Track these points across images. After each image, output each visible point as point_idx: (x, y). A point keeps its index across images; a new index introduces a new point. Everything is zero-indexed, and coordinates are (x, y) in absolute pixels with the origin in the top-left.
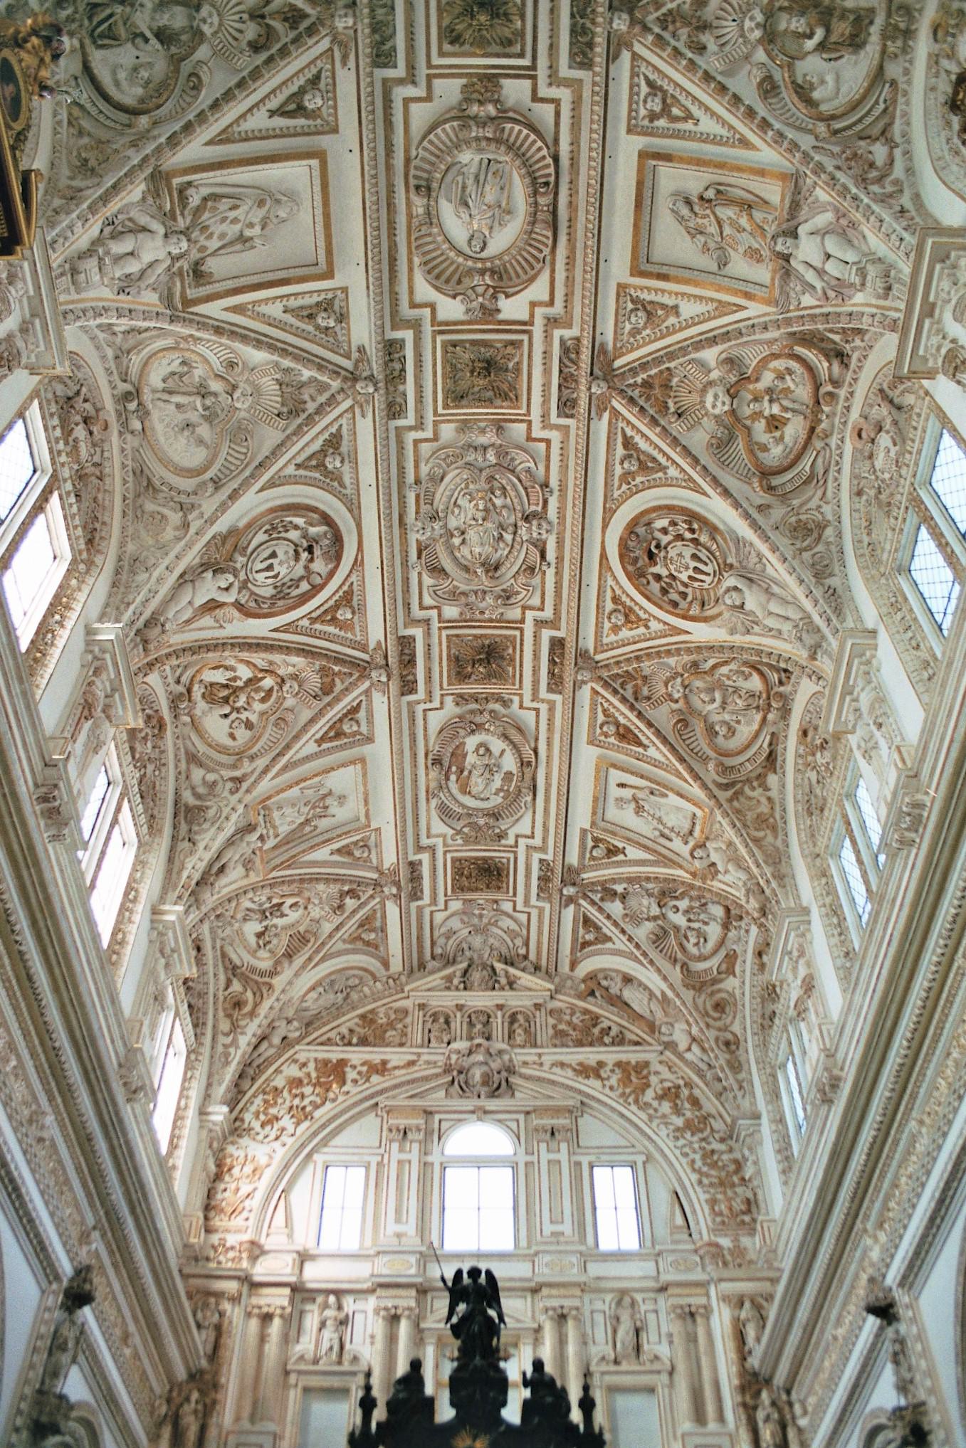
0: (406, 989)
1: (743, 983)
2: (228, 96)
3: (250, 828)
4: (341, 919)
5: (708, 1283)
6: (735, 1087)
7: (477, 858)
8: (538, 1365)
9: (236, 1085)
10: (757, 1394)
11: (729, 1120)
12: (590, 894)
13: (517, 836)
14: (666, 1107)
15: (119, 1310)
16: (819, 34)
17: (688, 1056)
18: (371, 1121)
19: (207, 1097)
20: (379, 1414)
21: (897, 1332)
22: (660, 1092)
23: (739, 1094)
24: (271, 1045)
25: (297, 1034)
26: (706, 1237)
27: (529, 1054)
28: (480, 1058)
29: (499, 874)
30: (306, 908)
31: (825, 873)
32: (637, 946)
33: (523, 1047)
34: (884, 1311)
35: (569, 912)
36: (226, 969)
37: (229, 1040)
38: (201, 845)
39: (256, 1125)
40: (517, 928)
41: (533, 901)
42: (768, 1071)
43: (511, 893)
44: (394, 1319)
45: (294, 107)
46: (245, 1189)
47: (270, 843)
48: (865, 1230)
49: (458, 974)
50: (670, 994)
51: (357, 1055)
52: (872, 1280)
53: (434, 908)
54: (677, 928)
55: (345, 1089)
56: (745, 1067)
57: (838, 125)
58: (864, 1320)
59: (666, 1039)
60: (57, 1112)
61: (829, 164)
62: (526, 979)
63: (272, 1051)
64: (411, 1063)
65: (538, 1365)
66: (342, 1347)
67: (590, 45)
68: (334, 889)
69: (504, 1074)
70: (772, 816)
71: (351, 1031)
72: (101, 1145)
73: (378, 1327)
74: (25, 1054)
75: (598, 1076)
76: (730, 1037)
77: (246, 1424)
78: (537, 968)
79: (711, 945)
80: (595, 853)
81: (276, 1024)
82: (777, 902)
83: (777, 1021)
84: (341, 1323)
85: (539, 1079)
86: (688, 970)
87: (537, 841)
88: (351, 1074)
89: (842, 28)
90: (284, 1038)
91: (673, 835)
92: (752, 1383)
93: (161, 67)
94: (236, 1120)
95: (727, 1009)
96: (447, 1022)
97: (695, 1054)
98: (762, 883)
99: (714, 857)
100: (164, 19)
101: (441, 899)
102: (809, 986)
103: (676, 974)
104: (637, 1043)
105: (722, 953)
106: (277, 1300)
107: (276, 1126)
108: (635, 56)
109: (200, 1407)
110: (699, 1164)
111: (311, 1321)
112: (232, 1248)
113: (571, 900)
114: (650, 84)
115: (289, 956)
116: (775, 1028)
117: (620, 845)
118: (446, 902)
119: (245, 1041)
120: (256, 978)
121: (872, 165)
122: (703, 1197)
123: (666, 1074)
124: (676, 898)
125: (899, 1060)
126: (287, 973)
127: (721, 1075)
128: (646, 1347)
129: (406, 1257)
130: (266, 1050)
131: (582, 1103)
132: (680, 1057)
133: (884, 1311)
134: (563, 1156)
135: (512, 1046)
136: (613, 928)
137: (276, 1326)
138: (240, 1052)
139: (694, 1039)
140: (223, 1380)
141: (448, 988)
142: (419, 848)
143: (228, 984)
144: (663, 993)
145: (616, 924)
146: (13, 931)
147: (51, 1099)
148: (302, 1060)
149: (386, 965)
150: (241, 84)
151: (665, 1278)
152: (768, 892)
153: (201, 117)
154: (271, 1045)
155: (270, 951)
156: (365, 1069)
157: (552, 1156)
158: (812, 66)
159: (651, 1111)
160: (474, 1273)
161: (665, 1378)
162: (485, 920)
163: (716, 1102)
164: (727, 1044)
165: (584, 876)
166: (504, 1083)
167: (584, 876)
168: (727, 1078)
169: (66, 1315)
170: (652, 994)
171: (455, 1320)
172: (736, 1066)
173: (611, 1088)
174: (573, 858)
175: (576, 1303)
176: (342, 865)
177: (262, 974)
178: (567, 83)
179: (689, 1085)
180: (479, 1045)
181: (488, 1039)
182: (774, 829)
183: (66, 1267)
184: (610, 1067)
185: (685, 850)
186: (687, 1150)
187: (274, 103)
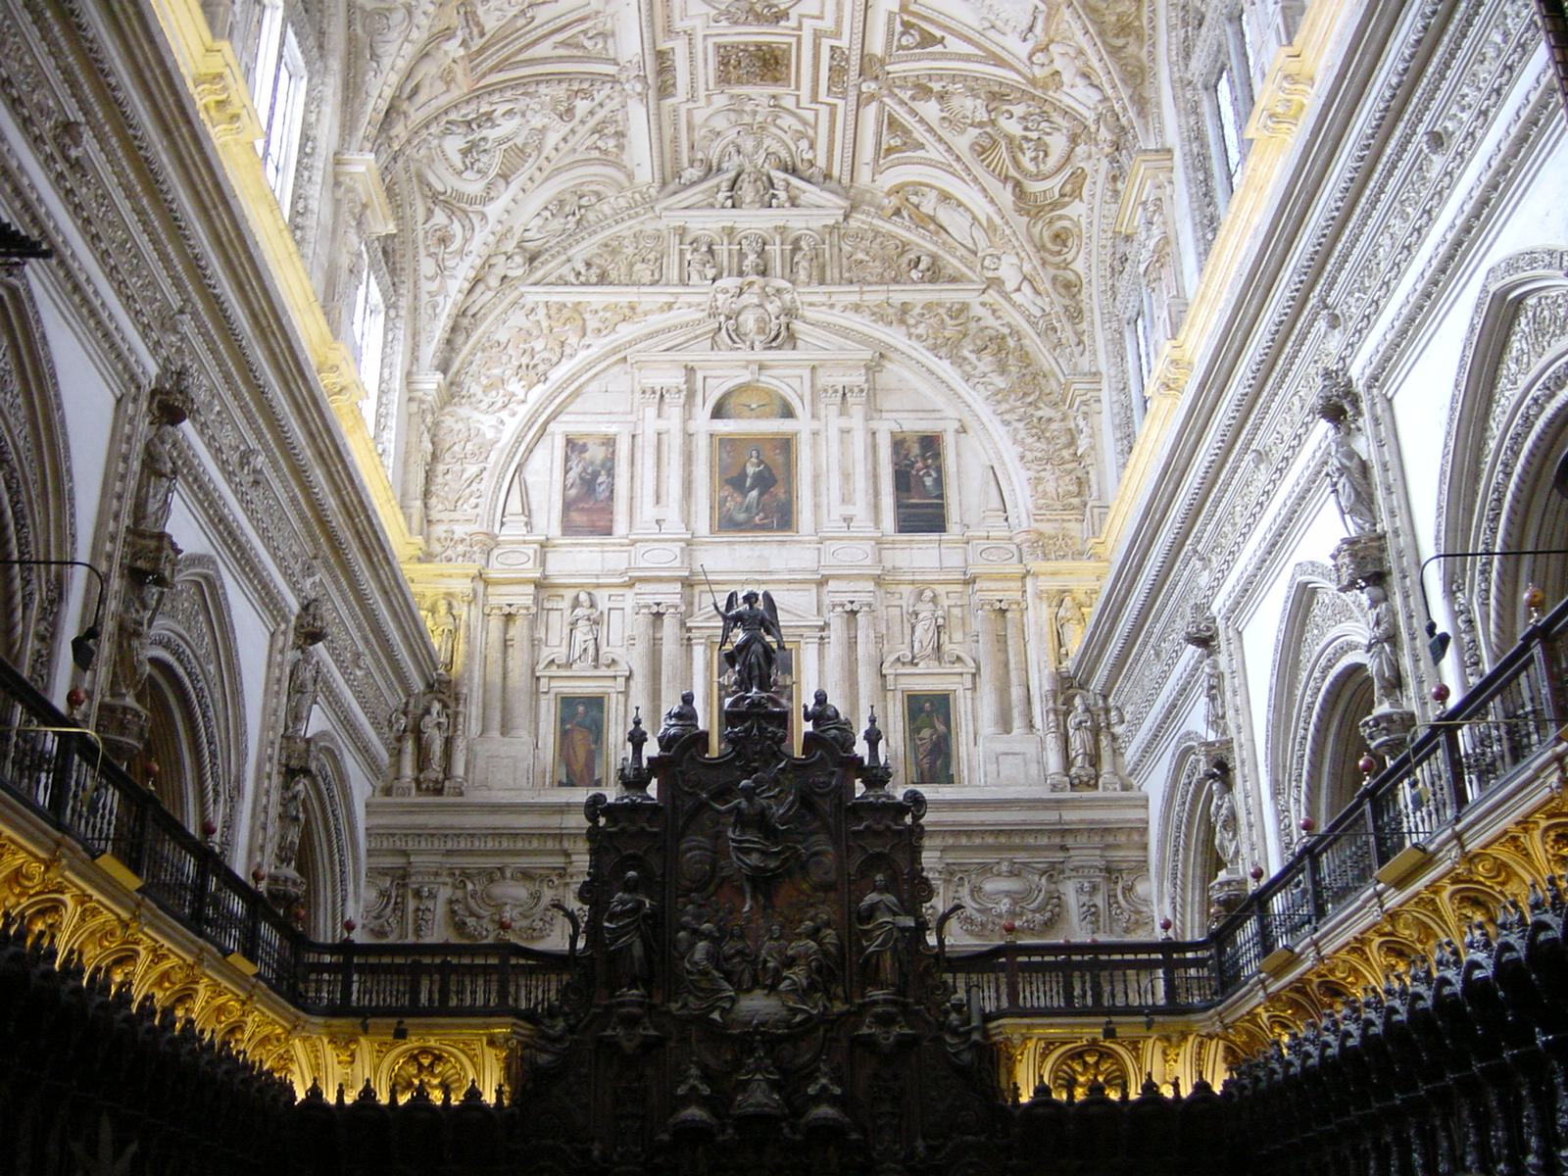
0: (657, 208)
1: (1092, 209)
3: (447, 34)
4: (570, 126)
5: (1024, 577)
6: (1073, 340)
7: (746, 44)
8: (821, 698)
9: (449, 341)
10: (1069, 701)
11: (1063, 380)
12: (896, 91)
13: (801, 16)
14: (986, 363)
15: (348, 633)
17: (1015, 297)
18: (619, 381)
19: (414, 357)
20: (651, 749)
21: (1215, 666)
22: (979, 342)
23: (1077, 350)
24: (489, 289)
25: (519, 272)
26: (1025, 526)
27: (816, 294)
28: (756, 301)
29: (777, 63)
30: (523, 115)
31: (1195, 110)
32: (958, 159)
33: (809, 284)
34: (1205, 641)
35: (870, 112)
36: (424, 196)
37: (434, 286)
38: (386, 62)
39: (476, 389)
40: (801, 128)
41: (823, 96)
42: (1115, 325)
43: (793, 87)
44: (659, 615)
46: (472, 470)
47: (477, 43)
48: (1195, 551)
49: (725, 186)
50: (997, 220)
51: (597, 297)
52: (1197, 607)
53: (691, 105)
54: (1010, 139)
55: (586, 341)
56: (1087, 314)
58: (1182, 650)
59: (990, 274)
60: (267, 448)
62: (811, 193)
63: (490, 294)
64: (670, 306)
65: (821, 698)
66: (597, 650)
68: (560, 91)
69: (783, 319)
70: (1138, 17)
71: (588, 265)
72: (318, 475)
73: (640, 626)
74: (228, 397)
75: (903, 322)
76: (1071, 276)
77: (495, 734)
78: (828, 176)
79: (1053, 161)
80: (904, 41)
81: (493, 261)
82: (1135, 137)
83: (1128, 265)
84: (596, 623)
85: (827, 326)
86: (1022, 191)
87: (827, 24)
88: (592, 323)
90: (505, 277)
91: (1008, 29)
92: (1067, 686)
94: (452, 384)
95: (1070, 244)
96: (710, 251)
97: (1024, 297)
98: (1117, 107)
99: (1058, 65)
101: (702, 93)
102: (1163, 254)
103: (1006, 196)
104: (953, 280)
105: (1068, 171)
106: (522, 598)
107: (501, 392)
109: (443, 720)
110: (1022, 434)
111: (558, 623)
112: (462, 541)
113: (872, 97)
115: (505, 177)
116: (1125, 275)
117: (938, 33)
118: (708, 97)
119: (456, 286)
120: (462, 205)
122: (1025, 474)
123: (990, 321)
124: (1010, 102)
125: (1241, 390)
126: (503, 200)
127: (1057, 325)
128: (947, 647)
129: (668, 545)
130: (482, 297)
131: (882, 356)
132: (1008, 299)
133: (1205, 641)
134: (856, 421)
135: (793, 283)
136: (927, 135)
137: (519, 630)
138: (450, 302)
139: (1025, 278)
140: (465, 690)
141: (712, 206)
142: (670, 31)
143: (430, 212)
144: (989, 219)
145: (931, 130)
146: (205, 276)
147: (260, 436)
148: (529, 306)
149: (630, 176)
151: (971, 571)
152: (1124, 121)
154: (489, 289)
155: (479, 172)
156: (608, 315)
157: (844, 422)
159: (968, 368)
160: (750, 598)
161: (968, 681)
162: (759, 118)
163: (1050, 358)
164: (1068, 286)
165: (889, 68)
166: (784, 333)
167: (889, 68)
168: (1063, 330)
169: (298, 654)
170: (975, 218)
171: (728, 647)
172: (1075, 315)
173: (919, 337)
174: (877, 46)
175: (866, 598)
176: (570, 59)
177: (472, 201)
179: (1015, 332)
180: (751, 284)
181: (764, 273)
182: (1140, 38)
183: (294, 605)
184: (918, 310)
185: (1023, 50)
186: (1007, 417)
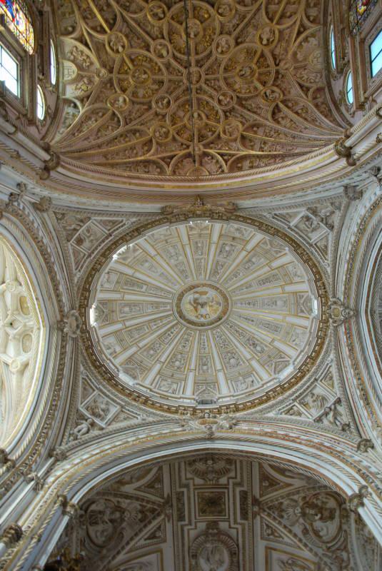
2: (132, 539)
16: (319, 516)
45: (153, 536)
57: (329, 545)
61: (329, 561)
67: (247, 513)
89: (326, 514)
93: (110, 530)
100: (113, 517)
108: (261, 517)
114: (267, 525)
121: (343, 561)
150: (136, 535)
153: (123, 548)
158: (318, 524)
178: (240, 524)
187: (146, 537)
